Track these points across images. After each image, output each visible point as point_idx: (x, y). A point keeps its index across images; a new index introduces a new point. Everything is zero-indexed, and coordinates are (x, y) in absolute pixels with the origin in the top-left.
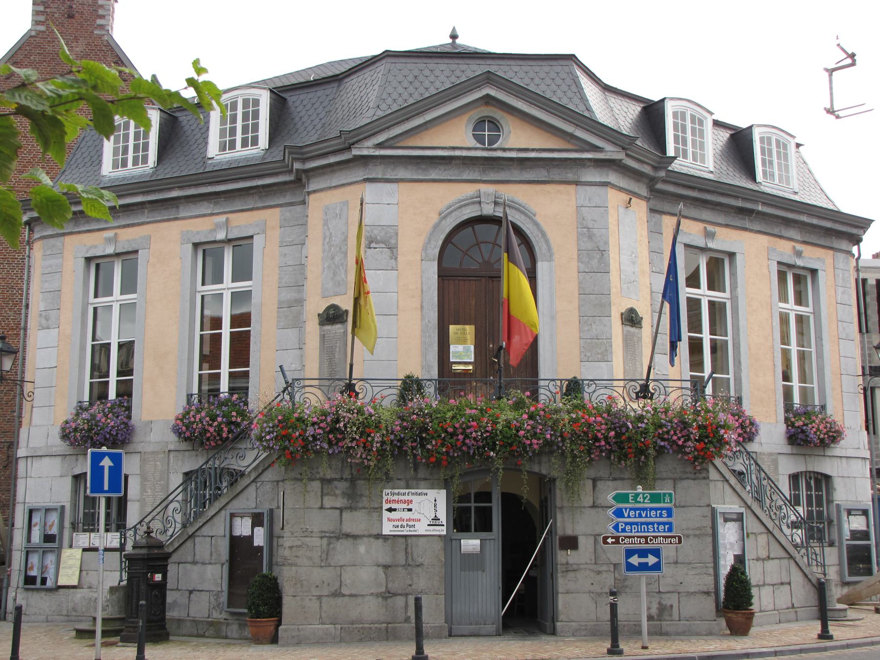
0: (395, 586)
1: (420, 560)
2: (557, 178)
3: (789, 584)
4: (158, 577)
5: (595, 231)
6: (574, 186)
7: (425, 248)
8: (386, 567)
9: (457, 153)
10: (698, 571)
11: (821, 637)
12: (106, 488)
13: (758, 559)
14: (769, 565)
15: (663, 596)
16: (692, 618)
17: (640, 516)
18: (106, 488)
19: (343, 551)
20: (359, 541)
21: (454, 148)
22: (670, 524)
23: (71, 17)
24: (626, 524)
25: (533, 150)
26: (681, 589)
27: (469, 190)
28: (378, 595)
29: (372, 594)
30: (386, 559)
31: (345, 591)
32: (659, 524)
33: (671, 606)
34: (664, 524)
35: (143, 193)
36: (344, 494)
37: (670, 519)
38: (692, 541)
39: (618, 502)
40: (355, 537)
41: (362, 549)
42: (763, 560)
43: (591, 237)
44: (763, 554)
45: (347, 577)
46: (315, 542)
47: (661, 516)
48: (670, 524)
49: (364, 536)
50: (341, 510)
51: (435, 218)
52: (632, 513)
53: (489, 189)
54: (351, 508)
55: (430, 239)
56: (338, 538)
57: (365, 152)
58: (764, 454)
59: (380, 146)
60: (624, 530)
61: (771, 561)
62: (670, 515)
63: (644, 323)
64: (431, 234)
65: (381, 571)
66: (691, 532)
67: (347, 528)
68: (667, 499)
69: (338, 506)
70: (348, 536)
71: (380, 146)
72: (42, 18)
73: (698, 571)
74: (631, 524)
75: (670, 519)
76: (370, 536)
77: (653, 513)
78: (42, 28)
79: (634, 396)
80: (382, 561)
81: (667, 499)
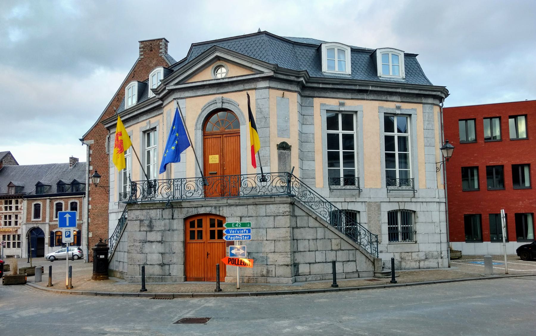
0: (165, 261)
1: (174, 251)
2: (247, 88)
3: (355, 261)
4: (102, 257)
5: (263, 109)
6: (254, 91)
7: (196, 125)
8: (162, 254)
9: (205, 83)
10: (284, 256)
11: (332, 286)
12: (68, 224)
13: (332, 250)
14: (340, 253)
15: (269, 266)
16: (281, 276)
17: (237, 233)
18: (68, 224)
19: (147, 248)
20: (153, 243)
21: (203, 81)
22: (250, 236)
23: (151, 51)
24: (231, 236)
25: (234, 77)
26: (276, 263)
27: (212, 98)
28: (159, 265)
29: (157, 264)
30: (163, 251)
31: (148, 263)
32: (245, 236)
33: (272, 271)
34: (247, 236)
35: (129, 114)
36: (148, 226)
37: (249, 234)
38: (282, 243)
39: (227, 227)
40: (152, 242)
41: (154, 247)
42: (336, 251)
43: (261, 112)
44: (335, 247)
45: (149, 257)
46: (137, 244)
47: (246, 233)
48: (250, 236)
49: (154, 242)
50: (146, 231)
51: (200, 111)
52: (233, 231)
53: (220, 96)
54: (151, 231)
55: (198, 121)
56: (145, 242)
57: (171, 88)
58: (371, 202)
59: (177, 84)
60: (230, 239)
61: (341, 252)
62: (249, 232)
63: (292, 149)
64: (198, 119)
65: (160, 255)
66: (281, 239)
67: (148, 239)
68: (248, 225)
69: (145, 230)
70: (149, 241)
71: (177, 84)
72: (142, 53)
73: (284, 256)
74: (233, 236)
75: (249, 234)
76: (157, 242)
77: (242, 231)
78: (142, 57)
79: (259, 180)
80: (161, 251)
81: (248, 225)
